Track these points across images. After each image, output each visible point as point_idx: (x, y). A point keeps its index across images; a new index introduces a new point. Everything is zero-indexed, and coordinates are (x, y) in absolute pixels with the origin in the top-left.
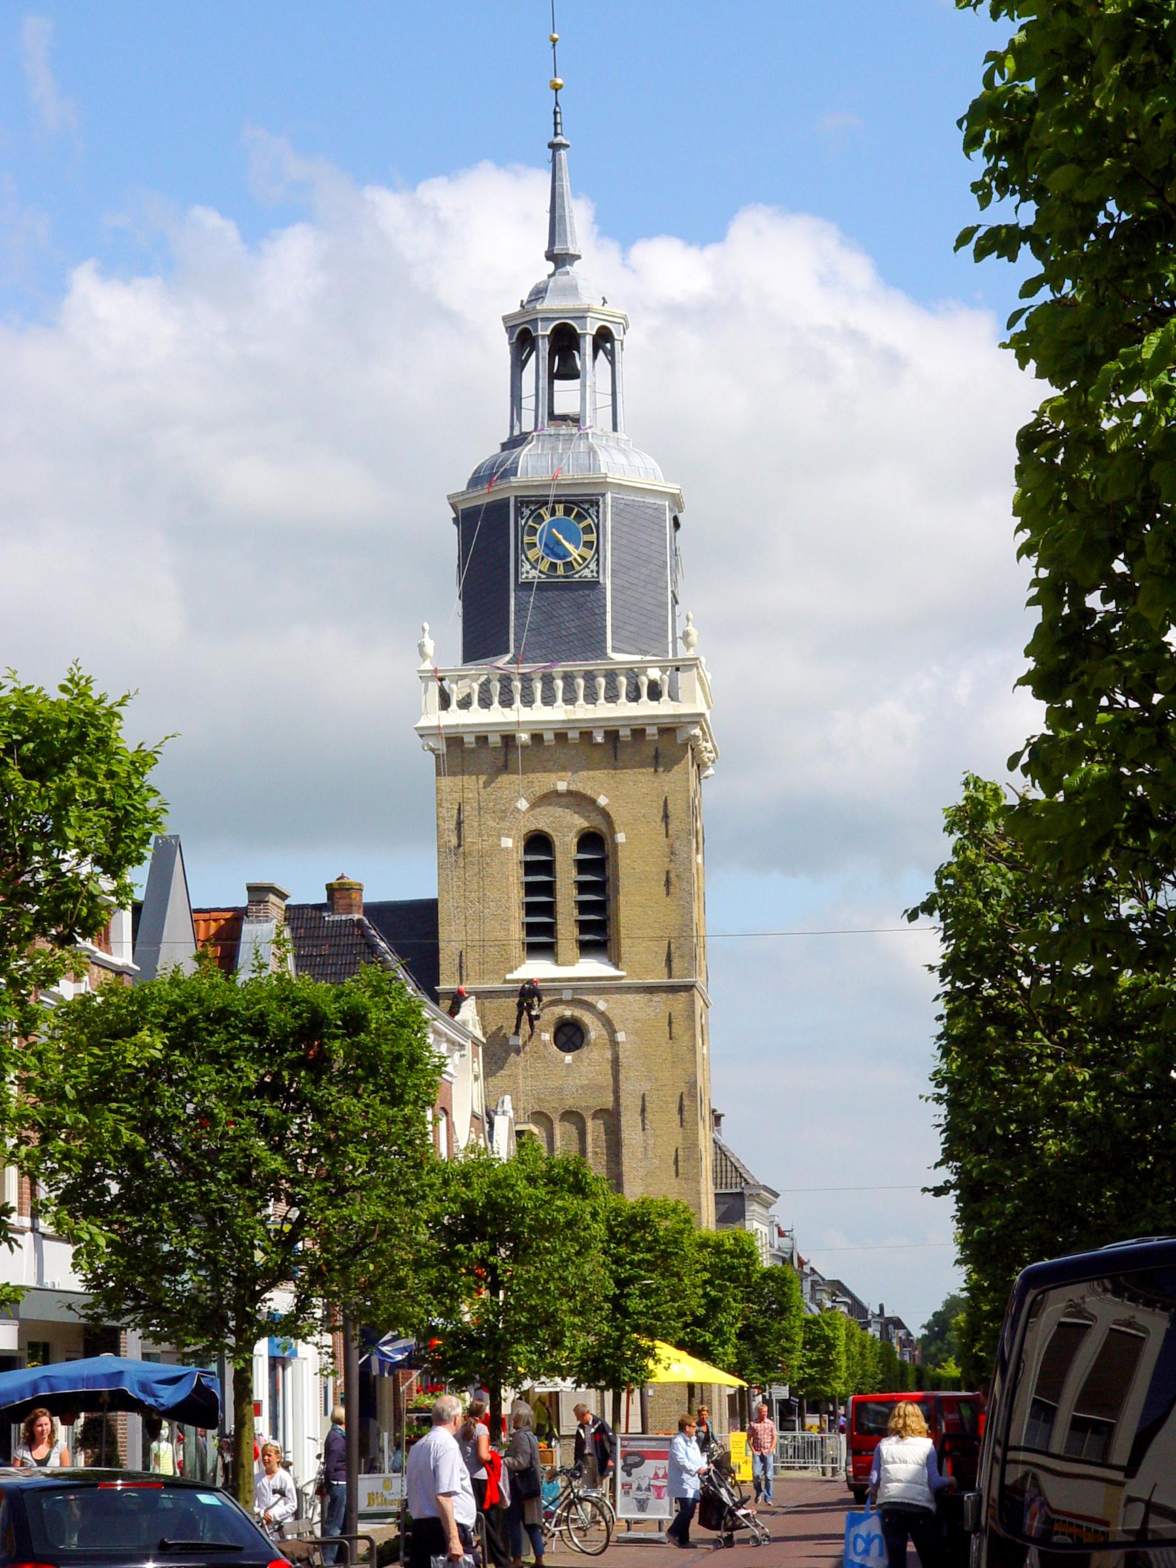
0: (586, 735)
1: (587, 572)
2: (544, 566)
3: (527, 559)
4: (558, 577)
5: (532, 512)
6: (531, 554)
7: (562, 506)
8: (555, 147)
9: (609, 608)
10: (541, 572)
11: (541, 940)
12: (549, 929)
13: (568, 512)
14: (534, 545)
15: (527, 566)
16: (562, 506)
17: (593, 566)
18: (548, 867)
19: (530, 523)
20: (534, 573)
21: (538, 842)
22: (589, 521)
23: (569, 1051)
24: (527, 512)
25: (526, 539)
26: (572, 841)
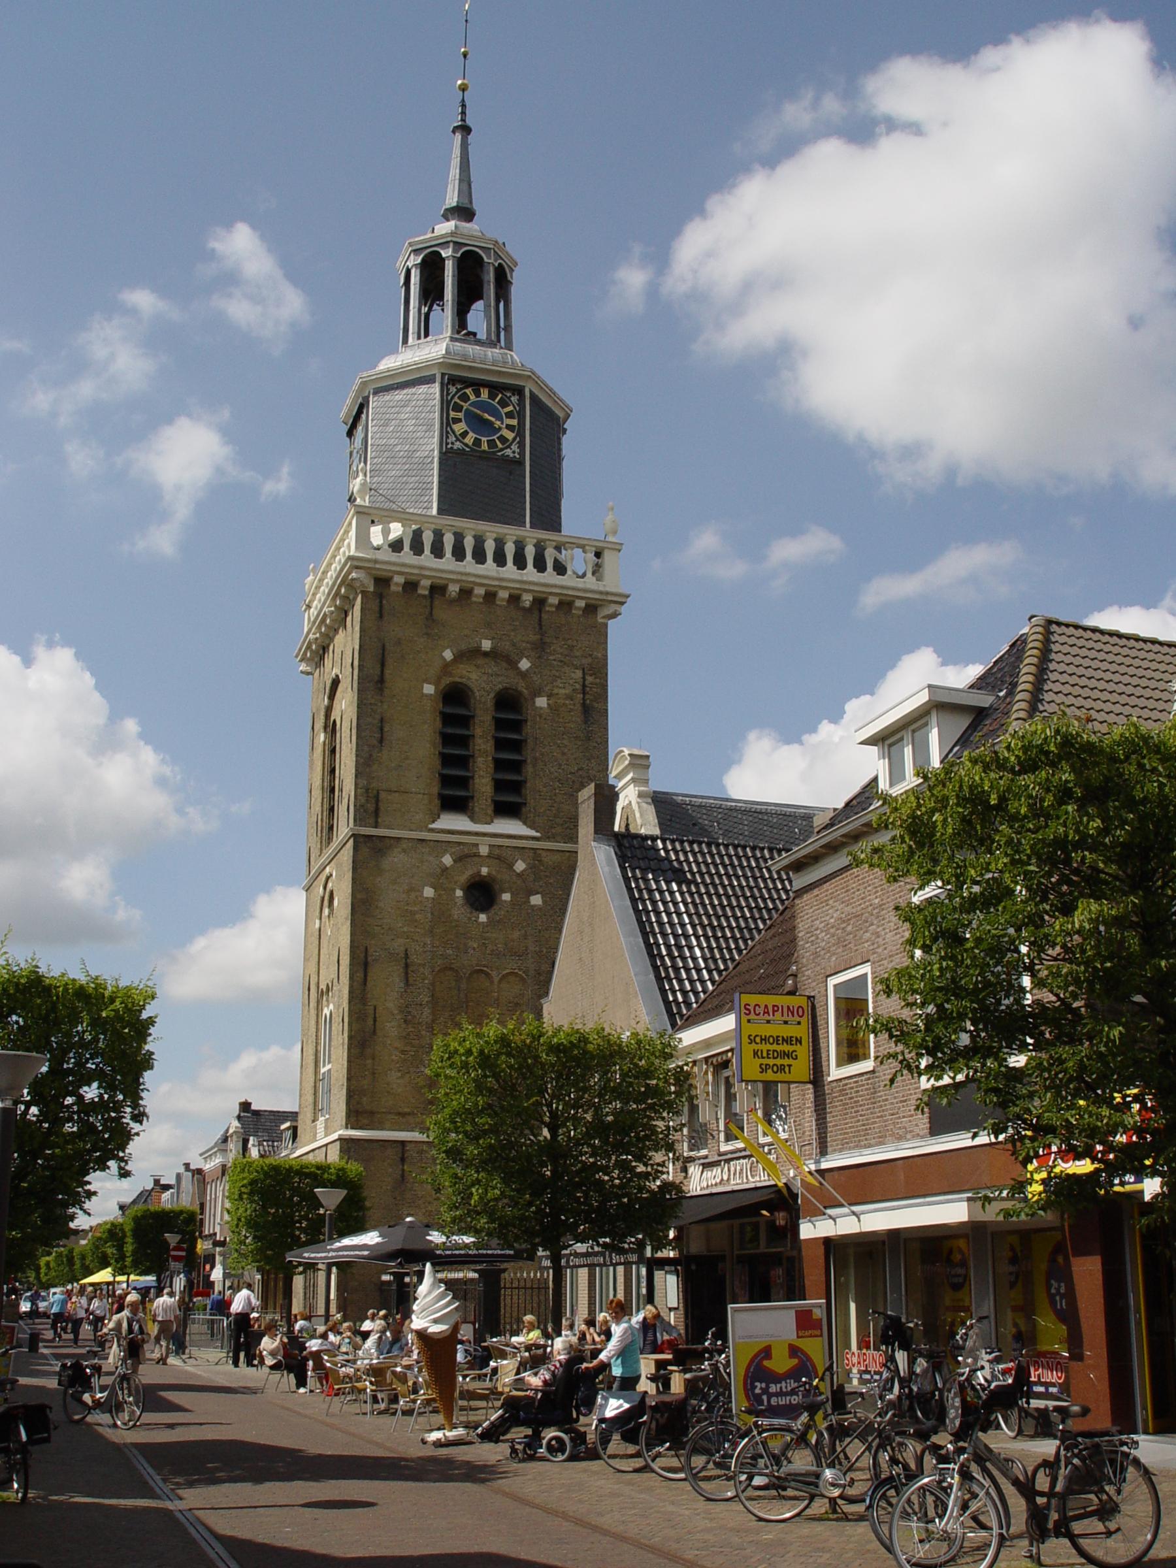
1: (508, 452)
3: (454, 432)
4: (484, 451)
5: (458, 390)
6: (459, 428)
7: (486, 391)
8: (465, 129)
9: (528, 489)
10: (466, 445)
11: (455, 799)
12: (464, 782)
13: (492, 396)
14: (459, 420)
15: (452, 439)
17: (515, 447)
18: (465, 721)
19: (456, 399)
20: (458, 445)
21: (455, 697)
22: (510, 408)
23: (483, 909)
25: (452, 414)
26: (489, 700)
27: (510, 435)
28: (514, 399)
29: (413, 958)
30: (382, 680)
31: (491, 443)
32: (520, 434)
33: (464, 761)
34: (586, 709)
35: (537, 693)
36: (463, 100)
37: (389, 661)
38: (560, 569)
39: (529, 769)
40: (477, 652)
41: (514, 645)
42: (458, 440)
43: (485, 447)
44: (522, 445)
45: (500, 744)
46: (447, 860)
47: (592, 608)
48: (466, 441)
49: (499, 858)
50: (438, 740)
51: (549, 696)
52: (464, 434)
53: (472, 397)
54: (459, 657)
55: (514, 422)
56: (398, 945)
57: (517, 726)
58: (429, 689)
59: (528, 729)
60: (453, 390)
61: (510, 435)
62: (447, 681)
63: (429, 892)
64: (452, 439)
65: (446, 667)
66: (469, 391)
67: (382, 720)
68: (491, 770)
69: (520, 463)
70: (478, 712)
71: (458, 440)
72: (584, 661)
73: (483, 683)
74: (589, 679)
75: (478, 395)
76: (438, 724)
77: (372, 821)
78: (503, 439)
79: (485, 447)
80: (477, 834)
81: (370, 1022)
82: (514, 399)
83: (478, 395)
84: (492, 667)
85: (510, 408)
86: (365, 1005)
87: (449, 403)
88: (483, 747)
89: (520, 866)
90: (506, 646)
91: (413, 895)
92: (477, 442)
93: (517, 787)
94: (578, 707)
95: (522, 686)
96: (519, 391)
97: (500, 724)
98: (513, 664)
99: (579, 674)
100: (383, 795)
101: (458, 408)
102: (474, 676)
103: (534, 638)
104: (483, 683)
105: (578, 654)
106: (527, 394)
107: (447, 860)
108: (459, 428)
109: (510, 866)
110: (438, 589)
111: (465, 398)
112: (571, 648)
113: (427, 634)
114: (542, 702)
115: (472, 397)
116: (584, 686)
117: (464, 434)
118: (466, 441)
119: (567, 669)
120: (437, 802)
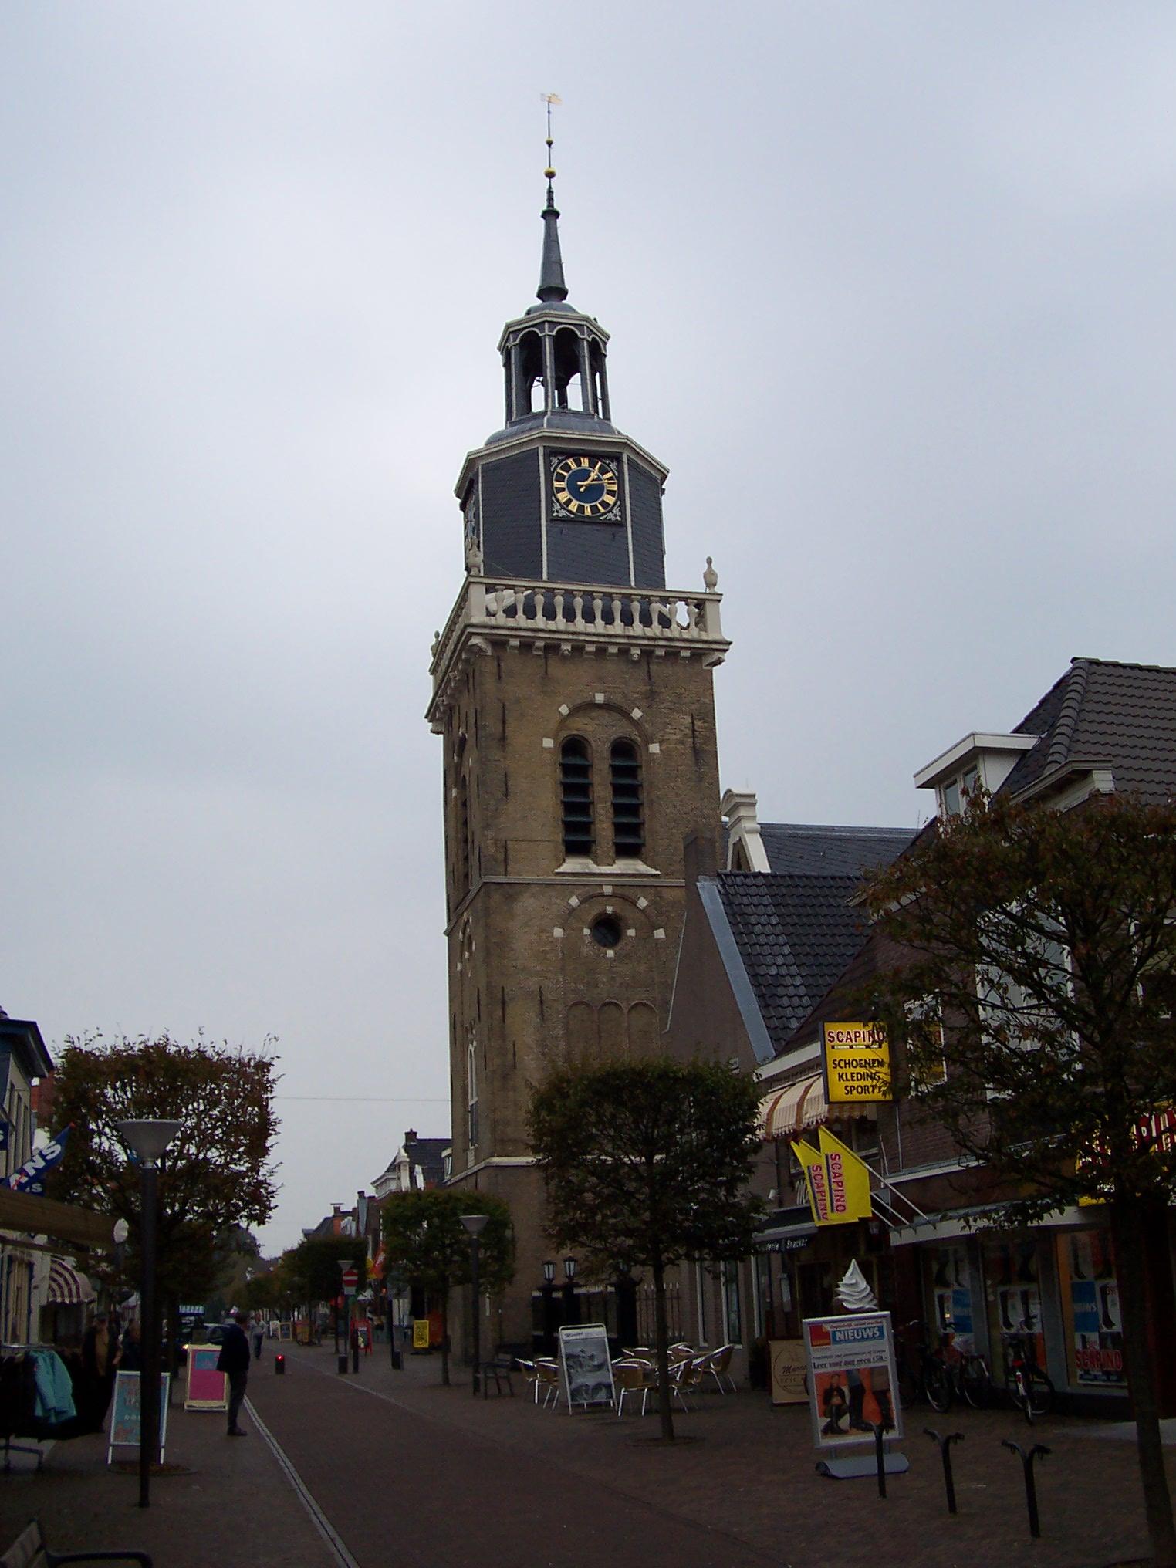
1: (610, 516)
11: (578, 843)
12: (586, 828)
14: (563, 489)
18: (584, 770)
20: (563, 513)
21: (573, 748)
22: (610, 474)
23: (612, 945)
24: (555, 461)
25: (556, 484)
27: (610, 500)
28: (613, 466)
29: (547, 995)
30: (503, 738)
31: (594, 509)
32: (620, 497)
33: (585, 808)
34: (696, 752)
35: (650, 740)
36: (550, 192)
37: (509, 719)
38: (665, 622)
39: (645, 813)
40: (592, 705)
41: (625, 696)
43: (588, 512)
44: (622, 509)
45: (618, 790)
46: (574, 901)
47: (697, 655)
48: (570, 508)
49: (623, 897)
50: (560, 790)
51: (661, 742)
52: (569, 502)
53: (574, 467)
54: (575, 711)
56: (533, 983)
57: (632, 771)
58: (548, 743)
59: (643, 774)
60: (555, 461)
61: (610, 500)
62: (565, 734)
63: (558, 932)
64: (557, 507)
65: (564, 720)
66: (570, 461)
67: (506, 775)
68: (611, 815)
69: (622, 525)
70: (596, 761)
72: (693, 707)
73: (600, 734)
74: (698, 723)
75: (579, 464)
76: (559, 775)
77: (502, 869)
78: (604, 504)
79: (588, 512)
80: (601, 875)
81: (510, 1056)
82: (613, 466)
83: (579, 464)
84: (607, 717)
85: (610, 474)
86: (504, 1040)
88: (602, 794)
89: (643, 903)
90: (618, 699)
91: (544, 936)
92: (581, 508)
93: (635, 829)
94: (689, 751)
95: (635, 735)
97: (616, 771)
98: (627, 715)
99: (688, 719)
100: (510, 845)
101: (560, 478)
102: (590, 728)
103: (645, 688)
104: (600, 734)
105: (687, 700)
106: (625, 460)
107: (574, 901)
108: (563, 497)
109: (634, 903)
110: (552, 648)
111: (567, 468)
112: (679, 696)
113: (545, 693)
114: (655, 748)
115: (574, 467)
116: (694, 730)
117: (569, 502)
118: (570, 508)
119: (676, 716)
120: (562, 848)
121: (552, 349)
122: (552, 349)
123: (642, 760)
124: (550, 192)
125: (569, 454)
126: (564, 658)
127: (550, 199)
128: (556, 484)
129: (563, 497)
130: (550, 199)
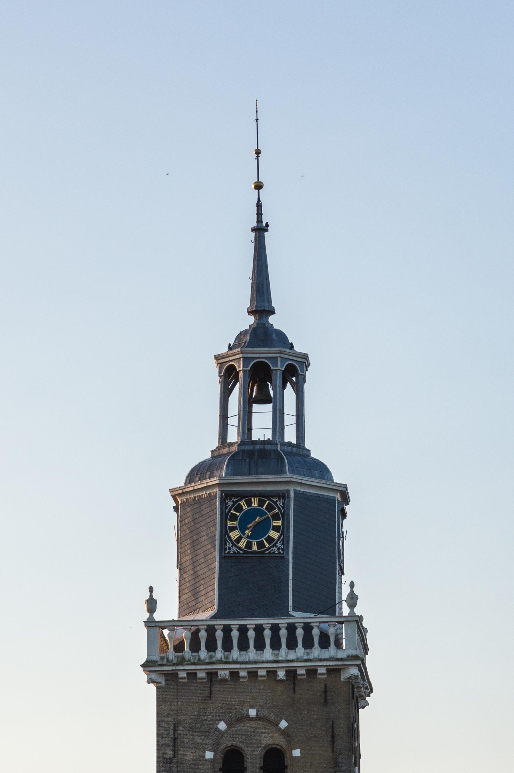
0: (272, 673)
2: (242, 544)
3: (230, 538)
4: (255, 552)
5: (234, 503)
7: (256, 499)
16: (256, 499)
24: (230, 503)
25: (230, 524)
27: (275, 535)
31: (260, 545)
36: (259, 206)
42: (234, 545)
43: (255, 548)
44: (285, 542)
52: (239, 540)
53: (245, 507)
55: (279, 523)
60: (230, 503)
61: (275, 535)
71: (234, 545)
78: (270, 540)
79: (255, 548)
87: (227, 515)
90: (265, 712)
96: (283, 496)
101: (234, 518)
111: (239, 509)
114: (296, 753)
115: (245, 507)
117: (239, 540)
121: (263, 365)
122: (263, 365)
123: (288, 762)
124: (259, 206)
125: (241, 495)
126: (224, 681)
127: (259, 214)
128: (230, 524)
129: (234, 535)
130: (259, 214)
